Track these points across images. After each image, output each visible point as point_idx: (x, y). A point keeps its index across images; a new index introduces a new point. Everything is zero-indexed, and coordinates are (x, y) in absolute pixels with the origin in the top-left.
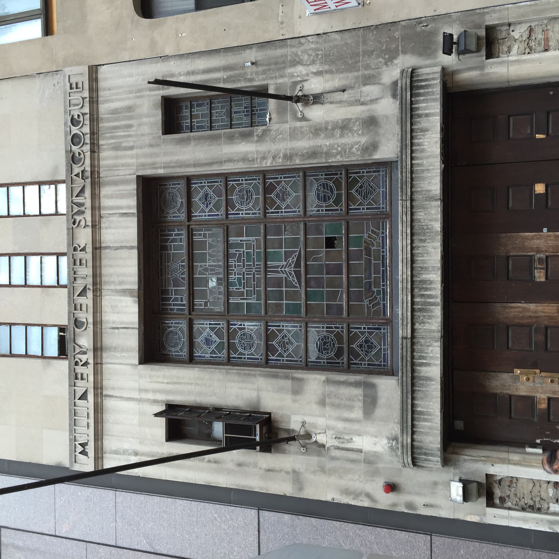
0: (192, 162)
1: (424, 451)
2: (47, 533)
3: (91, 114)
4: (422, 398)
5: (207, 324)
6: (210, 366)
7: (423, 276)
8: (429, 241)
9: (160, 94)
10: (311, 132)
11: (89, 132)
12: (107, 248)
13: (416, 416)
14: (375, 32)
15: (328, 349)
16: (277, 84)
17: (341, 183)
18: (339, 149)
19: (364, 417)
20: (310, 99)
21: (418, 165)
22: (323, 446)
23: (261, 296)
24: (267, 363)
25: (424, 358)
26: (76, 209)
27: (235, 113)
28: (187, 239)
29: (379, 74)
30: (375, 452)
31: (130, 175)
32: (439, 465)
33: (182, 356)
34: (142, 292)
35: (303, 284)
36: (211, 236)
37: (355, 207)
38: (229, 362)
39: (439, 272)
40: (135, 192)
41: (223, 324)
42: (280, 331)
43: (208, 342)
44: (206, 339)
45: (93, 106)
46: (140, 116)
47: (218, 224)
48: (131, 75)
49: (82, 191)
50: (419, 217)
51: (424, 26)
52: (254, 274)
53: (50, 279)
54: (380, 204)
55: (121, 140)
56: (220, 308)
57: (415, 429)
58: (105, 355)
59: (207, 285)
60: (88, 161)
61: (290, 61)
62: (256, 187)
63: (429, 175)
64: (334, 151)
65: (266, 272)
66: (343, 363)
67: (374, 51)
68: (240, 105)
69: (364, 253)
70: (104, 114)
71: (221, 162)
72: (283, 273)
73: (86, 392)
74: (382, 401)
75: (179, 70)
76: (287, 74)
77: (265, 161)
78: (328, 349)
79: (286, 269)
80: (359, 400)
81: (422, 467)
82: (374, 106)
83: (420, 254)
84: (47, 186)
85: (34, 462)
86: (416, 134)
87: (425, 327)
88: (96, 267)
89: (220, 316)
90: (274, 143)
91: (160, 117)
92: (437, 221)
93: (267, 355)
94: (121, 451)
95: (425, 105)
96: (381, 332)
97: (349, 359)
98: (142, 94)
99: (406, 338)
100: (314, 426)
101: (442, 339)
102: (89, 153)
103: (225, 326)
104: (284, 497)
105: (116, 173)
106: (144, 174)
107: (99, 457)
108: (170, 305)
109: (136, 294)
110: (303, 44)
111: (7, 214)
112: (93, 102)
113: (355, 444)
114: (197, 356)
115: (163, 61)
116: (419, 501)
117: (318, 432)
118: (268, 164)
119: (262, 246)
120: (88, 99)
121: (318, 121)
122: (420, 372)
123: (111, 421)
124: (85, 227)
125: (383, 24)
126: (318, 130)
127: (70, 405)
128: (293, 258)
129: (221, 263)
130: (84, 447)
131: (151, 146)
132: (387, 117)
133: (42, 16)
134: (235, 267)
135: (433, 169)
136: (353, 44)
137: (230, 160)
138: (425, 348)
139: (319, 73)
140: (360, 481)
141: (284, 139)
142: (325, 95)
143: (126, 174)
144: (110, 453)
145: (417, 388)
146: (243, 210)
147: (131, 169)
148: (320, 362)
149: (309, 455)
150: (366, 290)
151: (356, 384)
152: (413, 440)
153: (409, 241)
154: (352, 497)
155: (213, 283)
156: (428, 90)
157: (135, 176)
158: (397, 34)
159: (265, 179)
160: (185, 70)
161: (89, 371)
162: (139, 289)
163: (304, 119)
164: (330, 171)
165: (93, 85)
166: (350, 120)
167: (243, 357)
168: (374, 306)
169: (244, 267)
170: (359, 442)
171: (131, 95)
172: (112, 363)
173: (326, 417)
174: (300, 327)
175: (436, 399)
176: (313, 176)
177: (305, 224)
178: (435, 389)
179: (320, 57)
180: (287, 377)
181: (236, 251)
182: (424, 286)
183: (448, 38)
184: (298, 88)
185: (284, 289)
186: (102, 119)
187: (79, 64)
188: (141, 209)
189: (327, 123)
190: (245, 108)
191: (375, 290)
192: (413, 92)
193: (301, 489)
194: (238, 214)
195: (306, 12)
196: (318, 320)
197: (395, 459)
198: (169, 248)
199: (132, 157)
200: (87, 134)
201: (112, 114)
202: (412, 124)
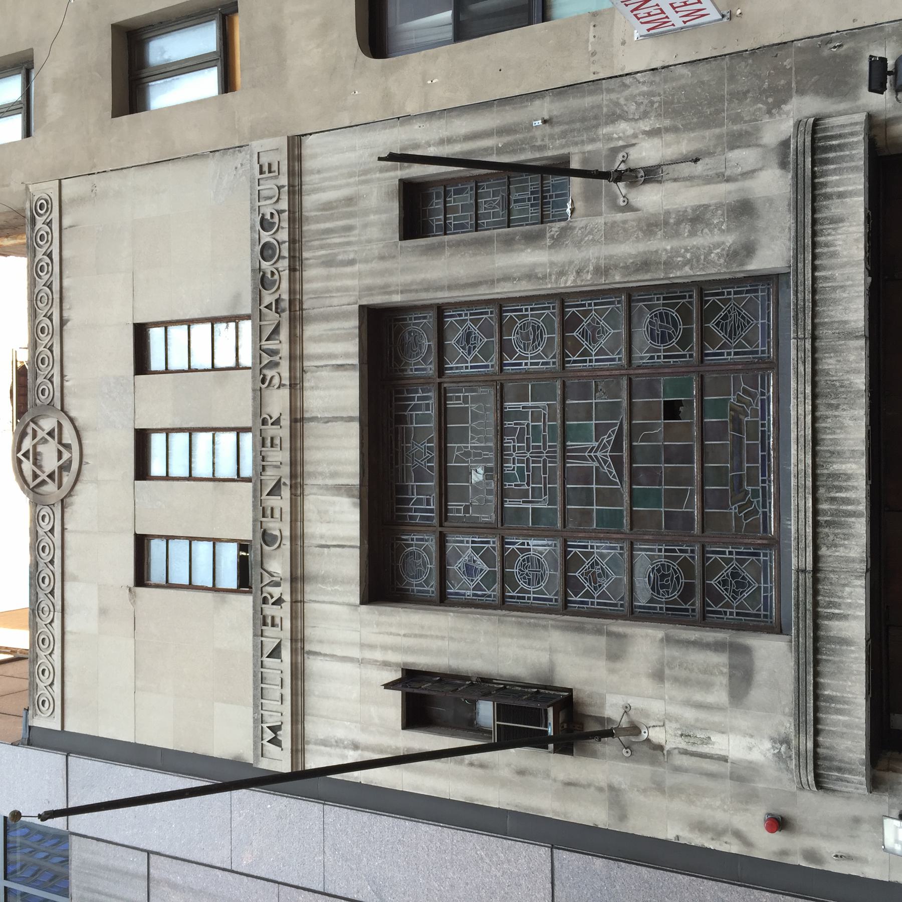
0: (446, 284)
1: (836, 763)
2: (218, 865)
3: (291, 211)
4: (833, 674)
5: (468, 542)
6: (473, 610)
7: (835, 466)
9: (397, 177)
10: (641, 229)
11: (286, 238)
13: (823, 704)
14: (750, 61)
15: (668, 587)
16: (584, 153)
17: (691, 312)
19: (730, 703)
20: (640, 175)
21: (826, 279)
22: (660, 748)
23: (555, 497)
24: (565, 607)
26: (266, 359)
27: (516, 201)
28: (437, 405)
29: (758, 129)
30: (751, 762)
32: (863, 789)
33: (428, 592)
34: (366, 489)
35: (626, 478)
36: (475, 400)
37: (715, 351)
38: (504, 604)
39: (863, 460)
40: (357, 331)
41: (493, 542)
42: (588, 555)
43: (470, 570)
44: (468, 567)
45: (294, 199)
46: (366, 213)
47: (487, 380)
48: (353, 149)
49: (276, 331)
50: (826, 367)
51: (835, 47)
52: (545, 461)
53: (226, 469)
54: (757, 346)
55: (336, 251)
56: (489, 517)
57: (820, 727)
58: (307, 588)
59: (468, 478)
60: (285, 285)
61: (606, 115)
62: (548, 321)
63: (845, 295)
64: (679, 259)
65: (564, 458)
66: (693, 610)
67: (748, 91)
68: (524, 189)
69: (729, 427)
70: (311, 211)
72: (593, 461)
73: (279, 646)
74: (761, 676)
75: (425, 138)
76: (601, 137)
77: (564, 278)
78: (668, 587)
79: (598, 454)
80: (722, 673)
81: (834, 791)
82: (748, 184)
83: (829, 428)
84: (224, 325)
85: (200, 752)
86: (822, 227)
87: (837, 554)
88: (296, 450)
89: (489, 528)
90: (579, 248)
92: (859, 372)
93: (566, 594)
94: (333, 740)
95: (838, 178)
96: (759, 560)
97: (704, 604)
98: (369, 177)
99: (804, 571)
100: (646, 714)
101: (868, 574)
102: (287, 271)
103: (498, 545)
104: (594, 829)
105: (327, 302)
106: (371, 303)
107: (298, 751)
108: (410, 510)
109: (357, 493)
110: (629, 87)
111: (163, 368)
113: (715, 746)
114: (451, 594)
115: (402, 124)
116: (828, 848)
117: (652, 723)
118: (568, 283)
119: (559, 416)
120: (286, 188)
121: (651, 210)
122: (828, 629)
123: (317, 693)
125: (764, 47)
126: (652, 226)
127: (255, 665)
128: (610, 436)
129: (491, 444)
130: (275, 733)
131: (382, 258)
132: (770, 200)
133: (219, 63)
134: (514, 451)
135: (852, 286)
136: (713, 83)
137: (507, 278)
138: (838, 588)
139: (654, 133)
140: (725, 811)
142: (664, 168)
143: (342, 303)
144: (316, 744)
145: (824, 657)
146: (527, 358)
147: (351, 296)
148: (655, 608)
149: (637, 761)
150: (733, 490)
151: (718, 647)
152: (816, 745)
153: (809, 408)
154: (710, 836)
155: (477, 476)
156: (842, 153)
157: (356, 307)
158: (787, 63)
159: (563, 307)
160: (437, 137)
161: (283, 613)
162: (361, 485)
163: (629, 207)
164: (672, 292)
165: (294, 166)
166: (706, 207)
167: (526, 595)
168: (747, 516)
169: (528, 450)
170: (720, 744)
171: (352, 180)
172: (318, 602)
173: (664, 699)
174: (622, 548)
175: (858, 677)
176: (644, 300)
177: (630, 379)
178: (856, 658)
179: (656, 105)
180: (599, 632)
181: (515, 424)
182: (836, 483)
183: (878, 67)
184: (620, 158)
185: (594, 486)
186: (307, 218)
187: (275, 134)
189: (668, 213)
190: (532, 193)
192: (815, 157)
193: (623, 817)
194: (520, 364)
195: (633, 35)
196: (650, 537)
197: (785, 776)
198: (408, 419)
199: (352, 276)
200: (284, 242)
201: (324, 209)
202: (814, 211)
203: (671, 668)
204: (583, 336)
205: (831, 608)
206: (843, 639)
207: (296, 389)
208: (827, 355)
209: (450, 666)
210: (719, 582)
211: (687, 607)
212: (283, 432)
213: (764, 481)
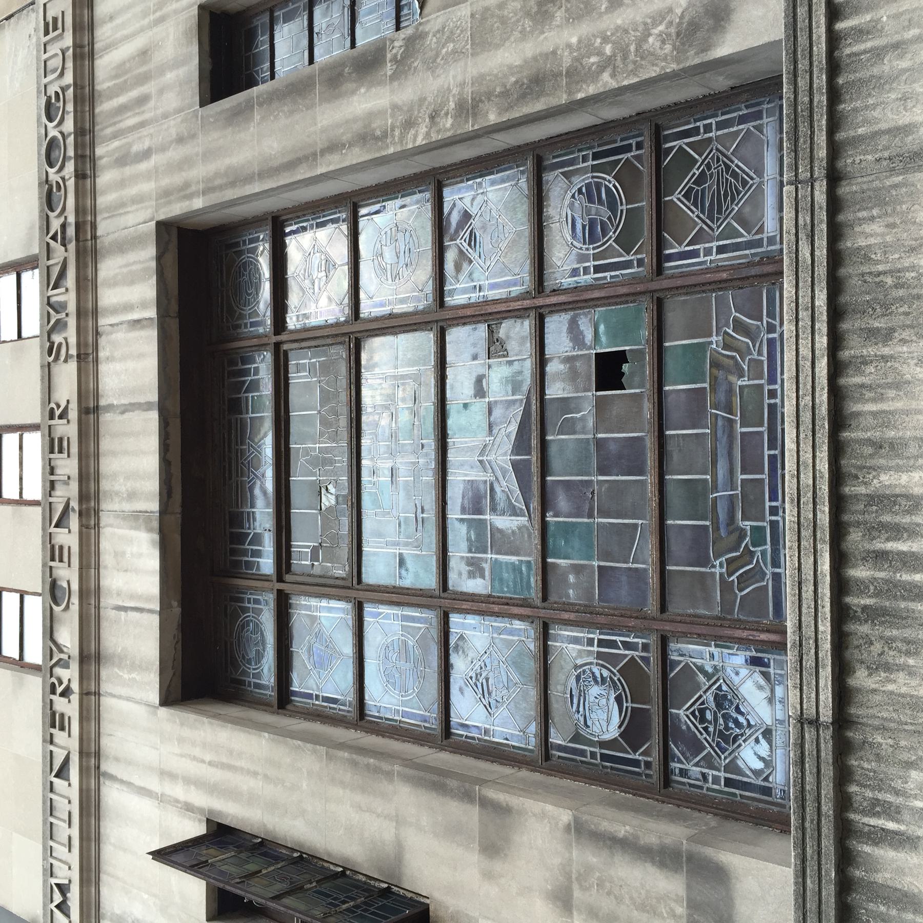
6: (317, 727)
7: (885, 478)
8: (905, 334)
10: (528, 14)
12: (110, 408)
18: (608, 49)
21: (861, 33)
25: (891, 811)
26: (54, 317)
31: (145, 222)
34: (176, 519)
35: (535, 504)
40: (153, 264)
45: (82, 66)
49: (62, 274)
50: (862, 242)
54: (761, 230)
55: (130, 138)
56: (340, 571)
58: (104, 673)
63: (904, 64)
64: (593, 59)
70: (104, 81)
77: (413, 132)
83: (870, 388)
84: (30, 272)
87: (890, 687)
88: (88, 457)
91: (196, 61)
97: (667, 756)
102: (73, 179)
109: (156, 524)
112: (82, 57)
122: (873, 865)
123: (112, 840)
124: (66, 361)
131: (180, 140)
137: (333, 147)
138: (893, 771)
141: (457, 54)
143: (137, 221)
148: (582, 753)
150: (716, 529)
151: (666, 858)
153: (822, 341)
155: (328, 500)
161: (69, 708)
162: (164, 510)
165: (82, 16)
168: (743, 581)
172: (114, 696)
180: (467, 796)
182: (887, 518)
188: (174, 307)
191: (747, 525)
196: (572, 616)
200: (70, 134)
201: (117, 76)
203: (584, 889)
204: (469, 245)
205: (877, 815)
206: (905, 894)
207: (87, 362)
208: (861, 214)
209: (265, 825)
210: (693, 713)
211: (637, 757)
212: (69, 430)
213: (774, 511)
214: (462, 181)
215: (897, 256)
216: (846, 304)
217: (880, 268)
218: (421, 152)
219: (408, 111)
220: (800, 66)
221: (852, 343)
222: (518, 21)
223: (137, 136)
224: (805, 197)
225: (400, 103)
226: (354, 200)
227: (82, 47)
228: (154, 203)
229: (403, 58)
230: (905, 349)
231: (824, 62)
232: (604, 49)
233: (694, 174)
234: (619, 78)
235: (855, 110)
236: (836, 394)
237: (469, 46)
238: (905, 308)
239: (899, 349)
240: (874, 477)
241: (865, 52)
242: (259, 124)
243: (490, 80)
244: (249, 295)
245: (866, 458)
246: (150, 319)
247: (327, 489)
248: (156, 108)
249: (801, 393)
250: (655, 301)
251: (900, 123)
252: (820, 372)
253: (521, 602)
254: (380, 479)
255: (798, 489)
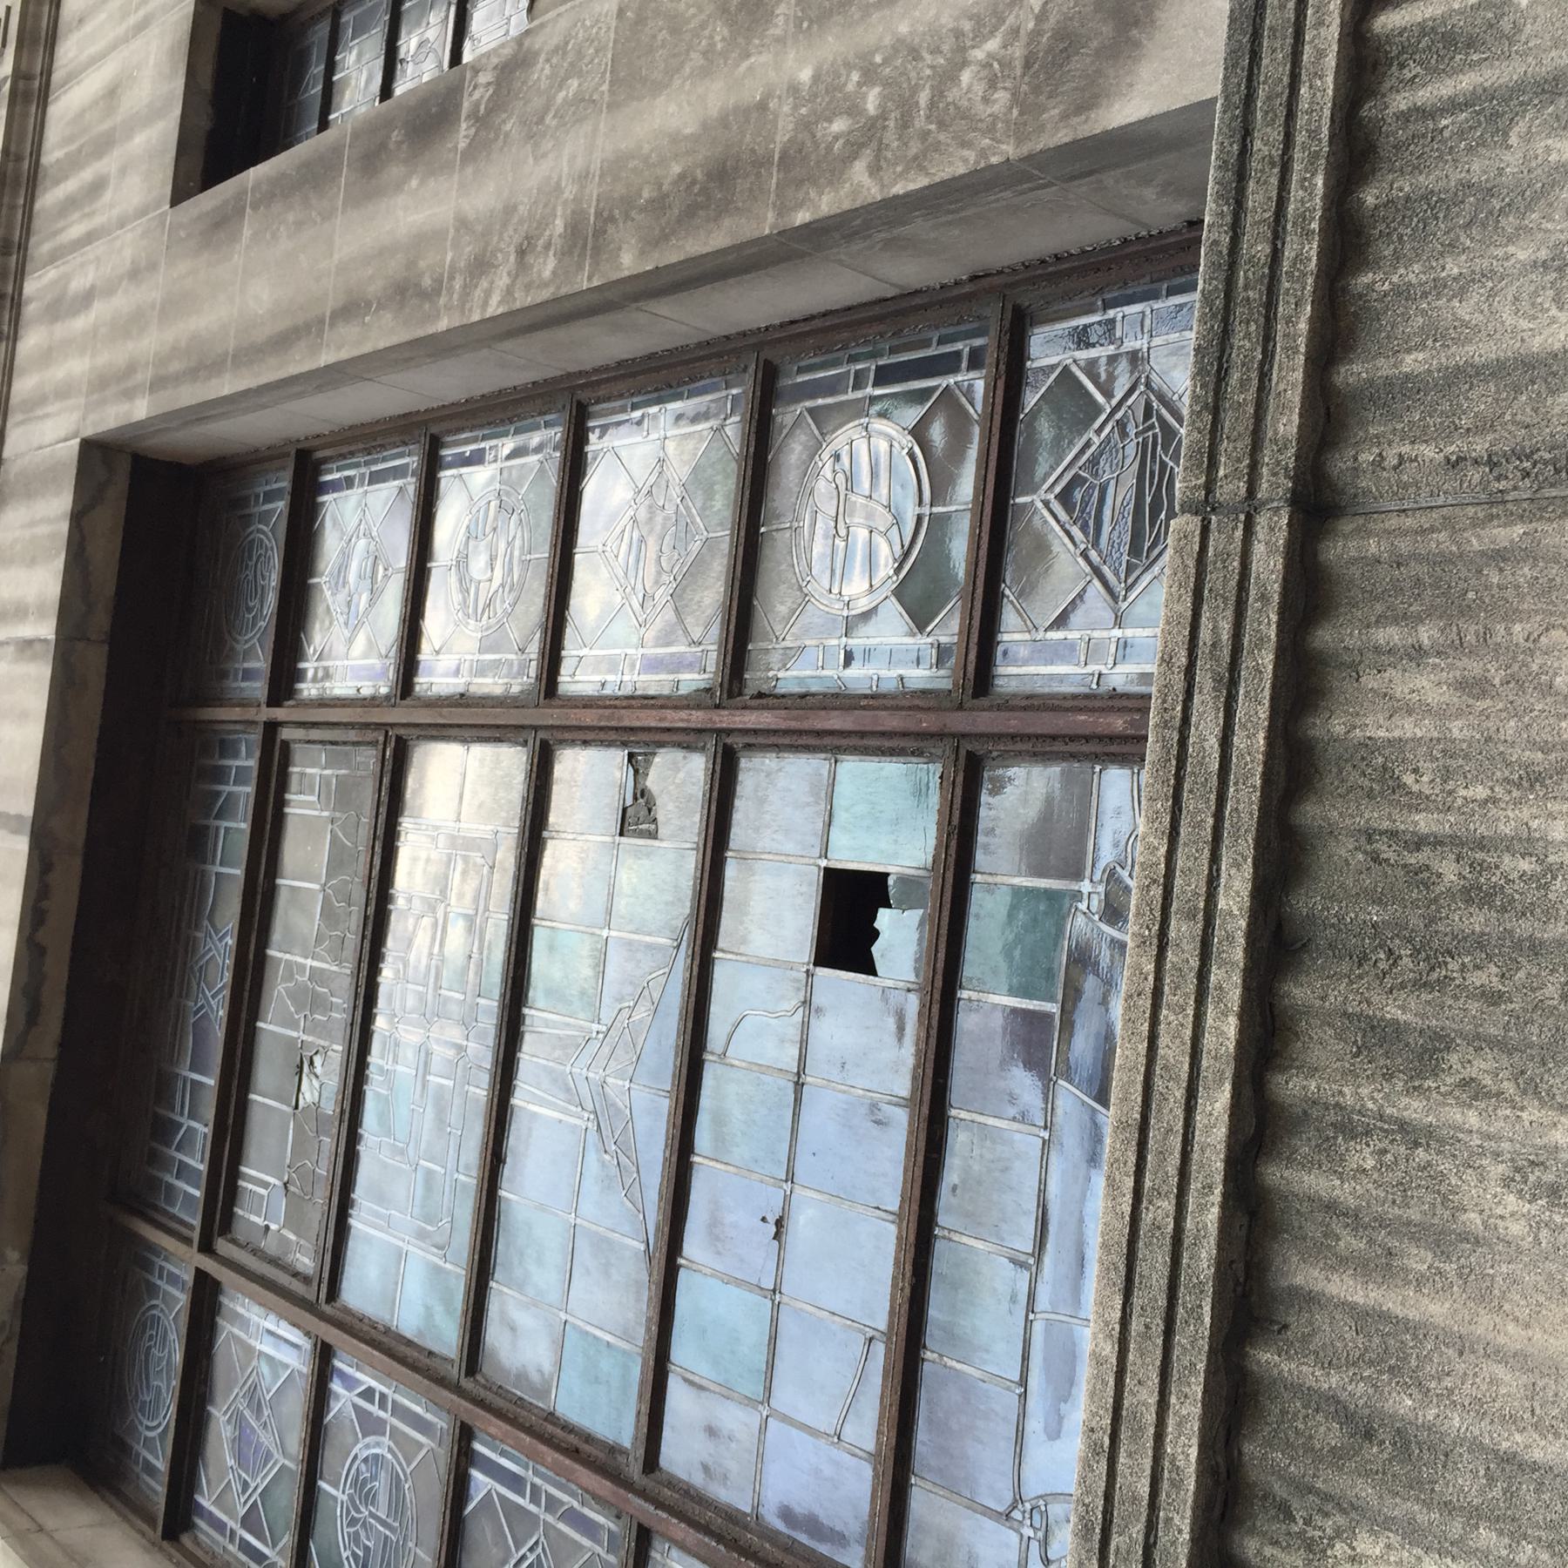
8: (1482, 1067)
21: (1447, 43)
31: (66, 440)
40: (64, 527)
45: (25, 115)
50: (1377, 728)
64: (839, 125)
71: (321, 321)
77: (484, 284)
83: (1354, 1219)
91: (178, 112)
112: (27, 97)
137: (352, 309)
153: (1224, 1030)
157: (75, 443)
165: (37, 17)
188: (101, 620)
214: (623, 410)
215: (1480, 792)
216: (1311, 918)
217: (1424, 823)
218: (510, 334)
219: (483, 235)
220: (1258, 144)
221: (1316, 1055)
222: (703, 26)
223: (79, 260)
224: (1225, 556)
225: (471, 216)
226: (434, 430)
227: (28, 77)
228: (82, 400)
229: (490, 111)
230: (1473, 1119)
231: (1325, 131)
232: (864, 97)
233: (1088, 444)
234: (887, 176)
235: (1403, 293)
236: (1252, 1213)
237: (605, 87)
238: (1487, 977)
239: (1455, 1115)
240: (1338, 1533)
241: (1453, 106)
242: (248, 247)
243: (634, 170)
244: (249, 610)
245: (1318, 1458)
246: (46, 641)
247: (311, 1063)
248: (112, 206)
249: (1148, 1184)
250: (962, 761)
251: (1536, 344)
252: (1208, 1129)
253: (601, 1455)
254: (400, 1068)
255: (1108, 1497)
